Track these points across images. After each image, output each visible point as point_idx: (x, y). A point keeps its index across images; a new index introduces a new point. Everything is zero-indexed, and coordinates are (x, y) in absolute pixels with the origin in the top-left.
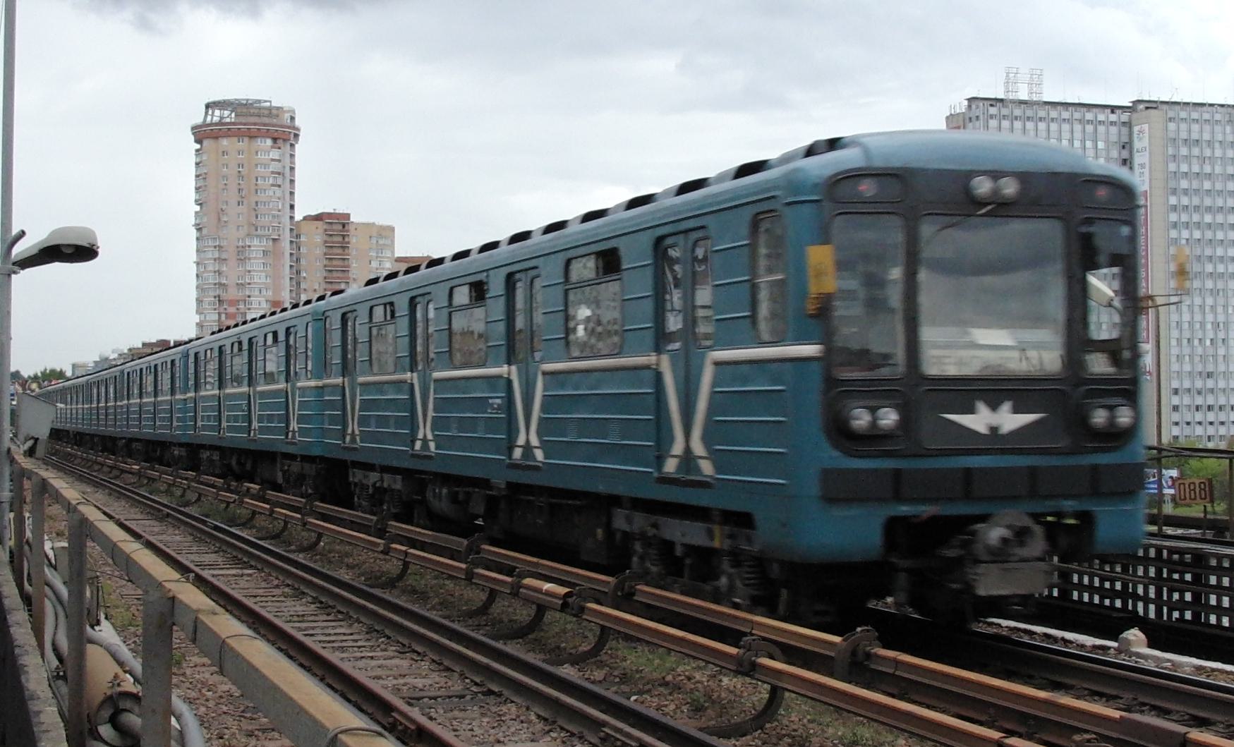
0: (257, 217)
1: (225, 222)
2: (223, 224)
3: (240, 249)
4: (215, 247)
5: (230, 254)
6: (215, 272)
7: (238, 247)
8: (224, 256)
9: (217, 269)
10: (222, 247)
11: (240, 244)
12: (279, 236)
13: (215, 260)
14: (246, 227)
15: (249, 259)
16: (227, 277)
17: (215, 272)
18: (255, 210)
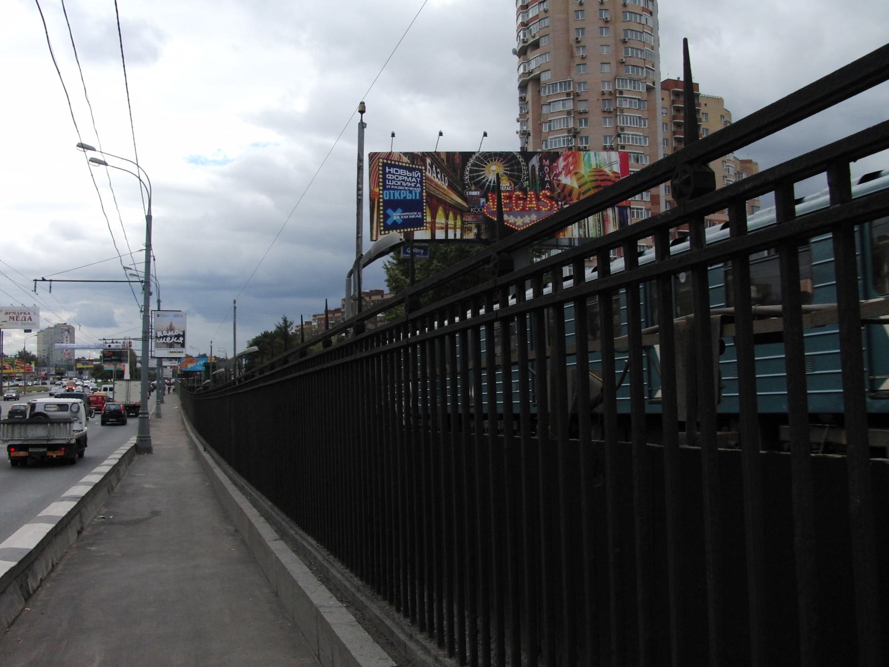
0: (627, 53)
1: (583, 58)
2: (578, 61)
3: (606, 97)
4: (568, 94)
5: (593, 105)
6: (569, 131)
7: (603, 93)
8: (582, 107)
9: (571, 126)
10: (578, 95)
11: (607, 88)
12: (654, 83)
13: (569, 113)
14: (613, 64)
15: (622, 111)
16: (587, 138)
17: (569, 131)
18: (624, 42)
